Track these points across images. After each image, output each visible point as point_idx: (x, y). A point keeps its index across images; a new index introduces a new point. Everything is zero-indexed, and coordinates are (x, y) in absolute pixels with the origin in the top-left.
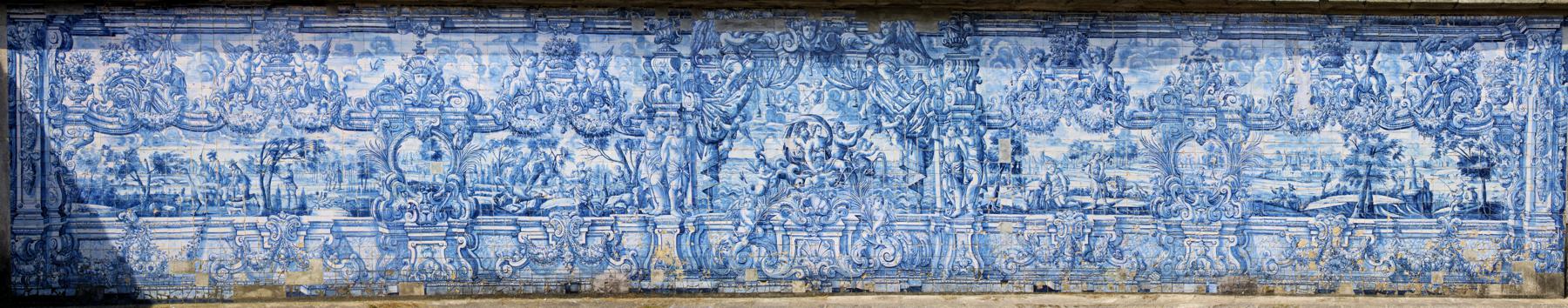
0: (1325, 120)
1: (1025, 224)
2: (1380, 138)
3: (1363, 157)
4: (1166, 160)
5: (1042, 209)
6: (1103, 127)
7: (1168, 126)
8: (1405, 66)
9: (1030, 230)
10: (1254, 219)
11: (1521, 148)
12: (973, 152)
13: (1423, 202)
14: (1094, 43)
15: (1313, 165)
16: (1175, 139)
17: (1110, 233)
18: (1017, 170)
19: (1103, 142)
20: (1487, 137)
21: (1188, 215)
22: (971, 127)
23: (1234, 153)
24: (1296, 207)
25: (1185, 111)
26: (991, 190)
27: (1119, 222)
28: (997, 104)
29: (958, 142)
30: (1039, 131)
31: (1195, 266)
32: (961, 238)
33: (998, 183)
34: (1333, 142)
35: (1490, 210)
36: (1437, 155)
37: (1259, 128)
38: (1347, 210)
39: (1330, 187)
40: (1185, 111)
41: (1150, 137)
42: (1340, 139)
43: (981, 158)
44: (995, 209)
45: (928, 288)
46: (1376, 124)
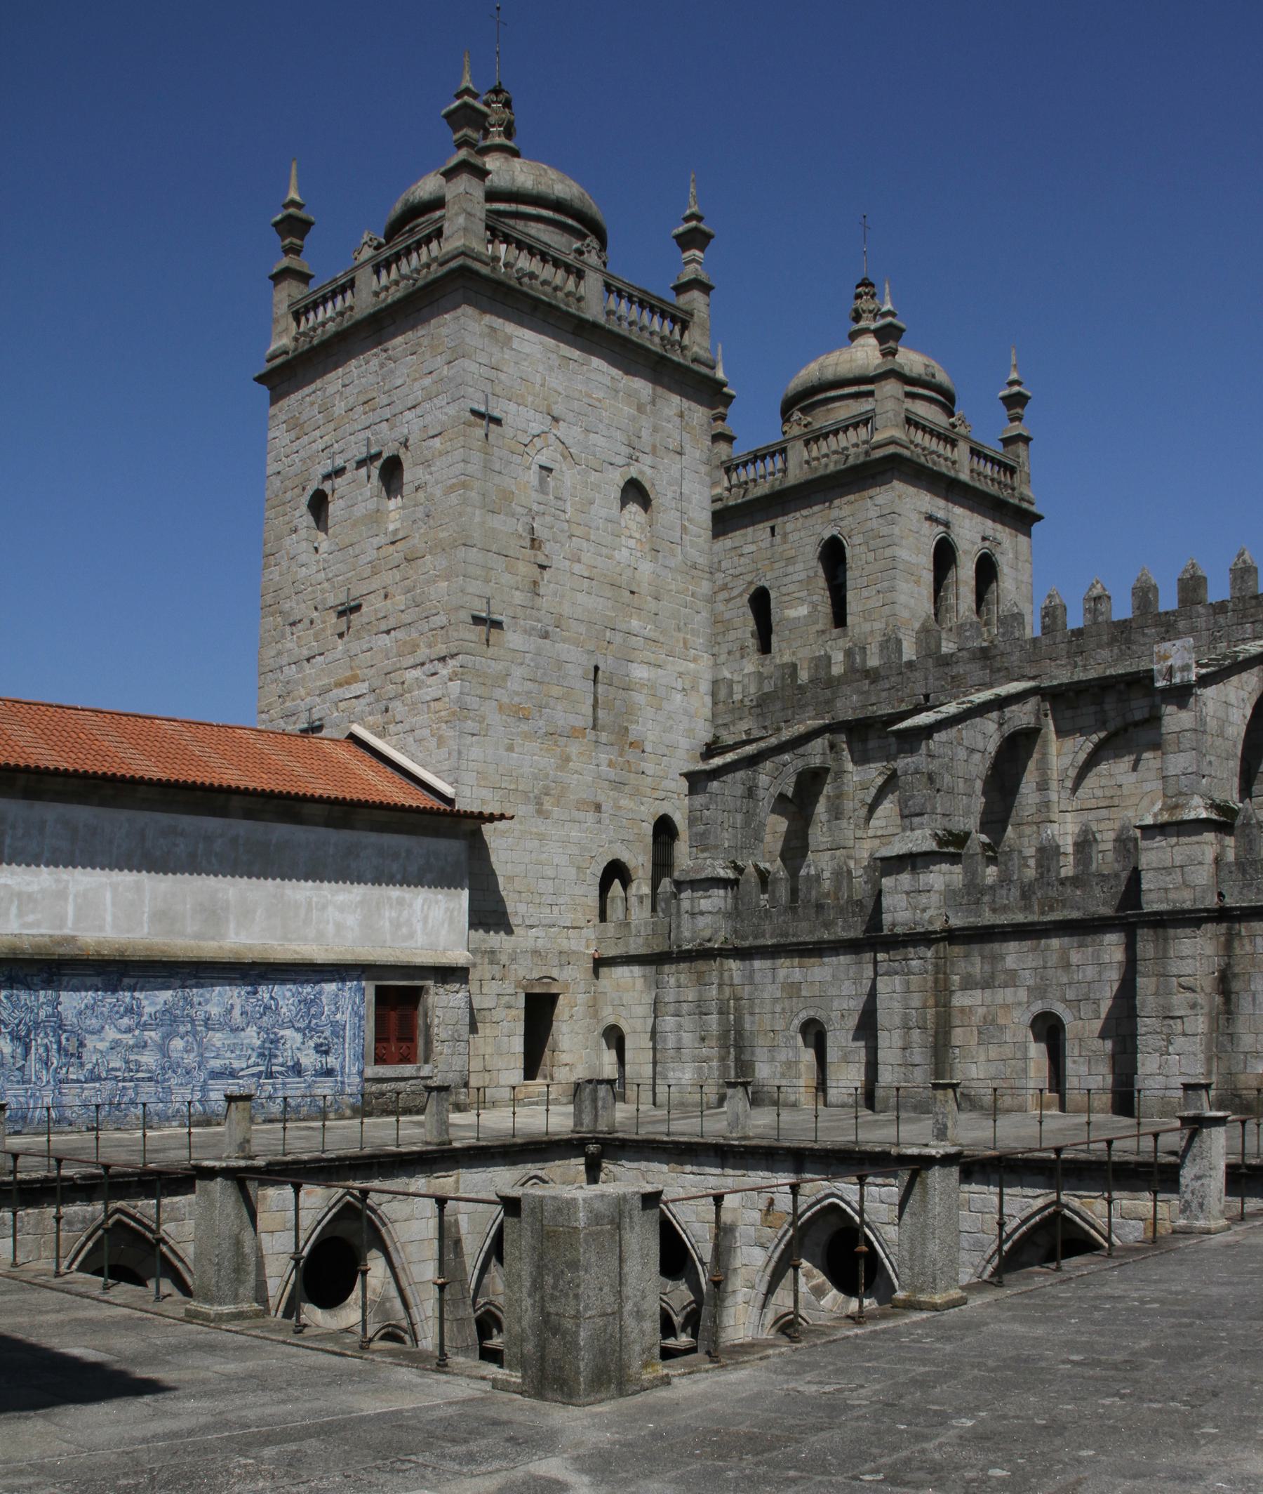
0: (248, 1025)
1: (83, 1089)
2: (276, 1034)
3: (267, 1045)
4: (163, 1050)
5: (93, 1080)
6: (129, 1030)
7: (164, 1029)
8: (288, 994)
9: (86, 1093)
10: (211, 1082)
11: (344, 1038)
12: (55, 1046)
13: (297, 1070)
14: (126, 981)
15: (241, 1050)
16: (168, 1037)
17: (131, 1093)
18: (80, 1058)
19: (129, 1039)
20: (327, 1034)
21: (174, 1082)
22: (54, 1031)
23: (200, 1044)
24: (233, 1074)
25: (174, 1020)
26: (64, 1070)
27: (136, 1086)
28: (70, 1017)
29: (46, 1041)
30: (93, 1033)
31: (178, 1111)
32: (46, 1099)
33: (68, 1065)
34: (252, 1036)
35: (329, 1072)
36: (303, 1043)
37: (213, 1030)
38: (259, 1075)
39: (251, 1062)
40: (174, 1020)
41: (153, 1036)
42: (255, 1035)
43: (59, 1050)
44: (68, 1081)
45: (25, 1131)
46: (273, 1026)
